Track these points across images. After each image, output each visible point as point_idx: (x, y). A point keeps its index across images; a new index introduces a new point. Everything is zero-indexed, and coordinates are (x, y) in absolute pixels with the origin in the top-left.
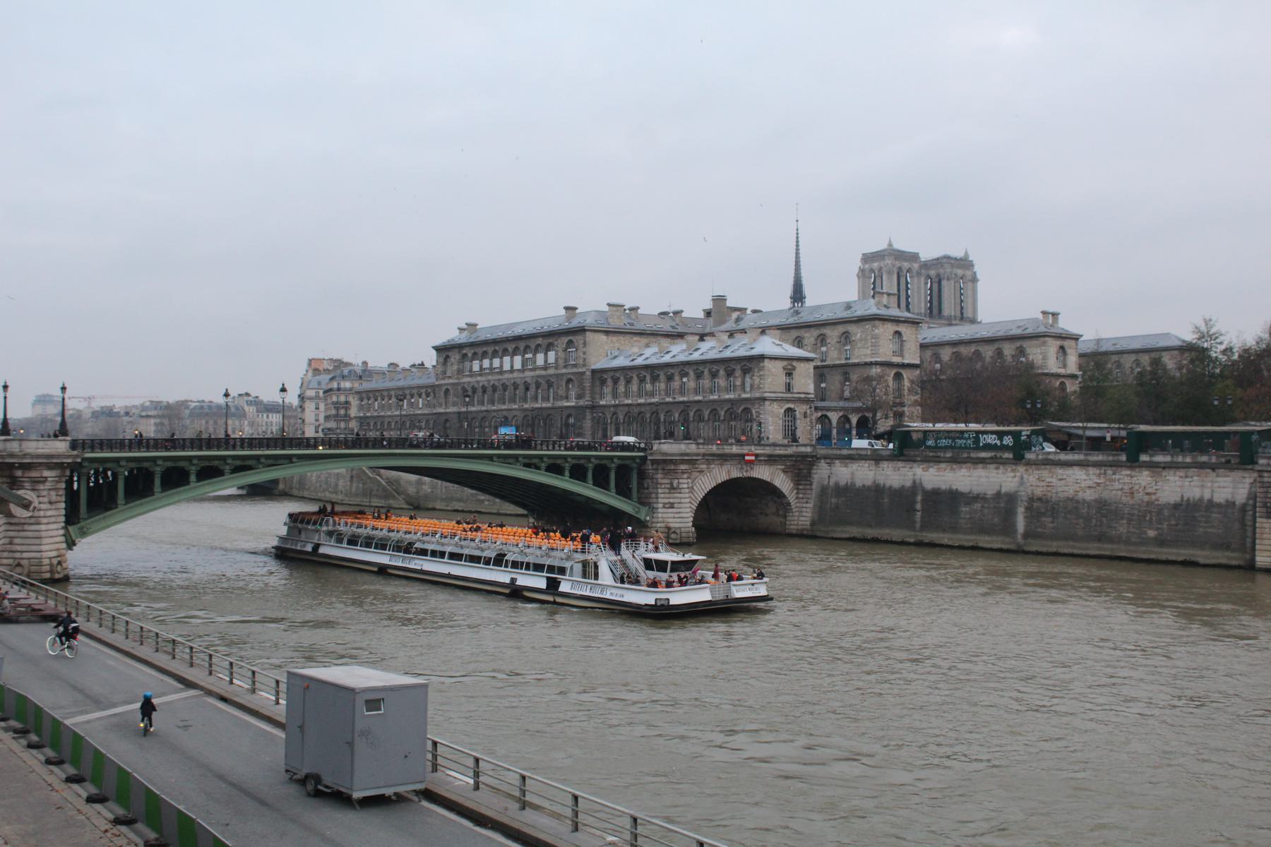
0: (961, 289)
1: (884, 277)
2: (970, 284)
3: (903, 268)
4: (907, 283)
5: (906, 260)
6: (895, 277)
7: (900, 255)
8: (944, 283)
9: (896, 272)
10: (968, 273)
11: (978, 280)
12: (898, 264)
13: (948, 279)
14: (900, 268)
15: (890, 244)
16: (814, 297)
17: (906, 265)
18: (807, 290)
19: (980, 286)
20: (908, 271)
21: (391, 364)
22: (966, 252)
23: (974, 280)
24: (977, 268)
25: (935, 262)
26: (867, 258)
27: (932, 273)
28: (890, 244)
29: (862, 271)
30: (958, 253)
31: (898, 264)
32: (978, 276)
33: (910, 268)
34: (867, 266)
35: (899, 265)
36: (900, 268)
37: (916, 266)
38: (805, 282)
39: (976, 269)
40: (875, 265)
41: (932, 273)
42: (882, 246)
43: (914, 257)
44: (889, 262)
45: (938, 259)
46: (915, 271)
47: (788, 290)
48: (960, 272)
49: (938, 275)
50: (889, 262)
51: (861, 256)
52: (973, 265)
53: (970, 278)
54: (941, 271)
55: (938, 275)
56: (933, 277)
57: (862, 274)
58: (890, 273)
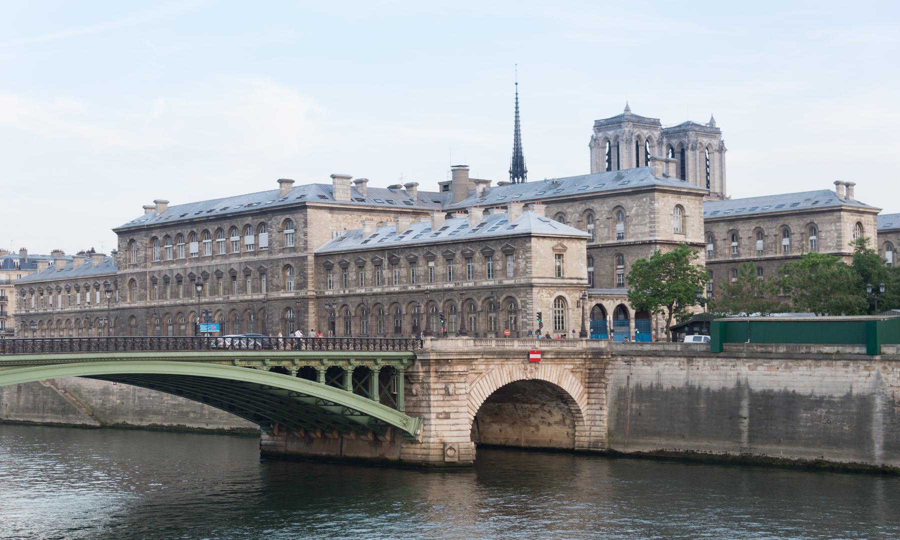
0: (707, 160)
2: (717, 154)
3: (643, 137)
4: (647, 154)
5: (645, 128)
7: (639, 121)
8: (689, 154)
9: (634, 141)
10: (715, 142)
11: (726, 150)
12: (637, 132)
13: (693, 149)
14: (639, 137)
15: (627, 109)
16: (535, 173)
17: (645, 133)
18: (528, 164)
19: (728, 156)
20: (647, 140)
21: (55, 251)
22: (712, 118)
23: (721, 149)
24: (726, 137)
25: (678, 129)
26: (600, 126)
27: (675, 142)
28: (627, 109)
29: (594, 140)
30: (702, 120)
31: (637, 132)
32: (726, 145)
34: (600, 134)
36: (639, 137)
37: (656, 134)
38: (526, 153)
39: (723, 137)
40: (611, 133)
41: (675, 142)
43: (654, 124)
45: (679, 126)
46: (655, 140)
47: (508, 164)
48: (705, 141)
49: (681, 144)
51: (593, 123)
52: (720, 133)
53: (717, 148)
54: (685, 140)
55: (681, 144)
56: (675, 147)
57: (594, 143)
58: (629, 142)
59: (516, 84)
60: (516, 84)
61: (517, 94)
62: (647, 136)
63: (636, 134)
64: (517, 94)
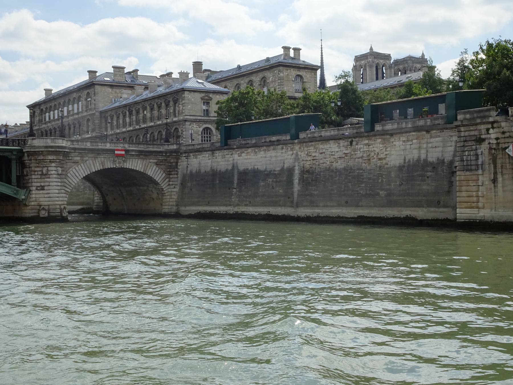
1: (367, 69)
3: (380, 64)
4: (383, 73)
5: (381, 59)
6: (375, 69)
9: (375, 66)
12: (376, 61)
15: (371, 49)
17: (382, 62)
20: (383, 66)
28: (371, 49)
31: (376, 61)
33: (384, 64)
34: (358, 63)
35: (377, 62)
41: (401, 67)
42: (365, 50)
43: (388, 57)
44: (371, 60)
45: (404, 58)
50: (371, 60)
55: (404, 68)
58: (371, 66)
59: (321, 40)
60: (321, 40)
61: (322, 46)
62: (383, 63)
63: (376, 62)
64: (322, 46)
